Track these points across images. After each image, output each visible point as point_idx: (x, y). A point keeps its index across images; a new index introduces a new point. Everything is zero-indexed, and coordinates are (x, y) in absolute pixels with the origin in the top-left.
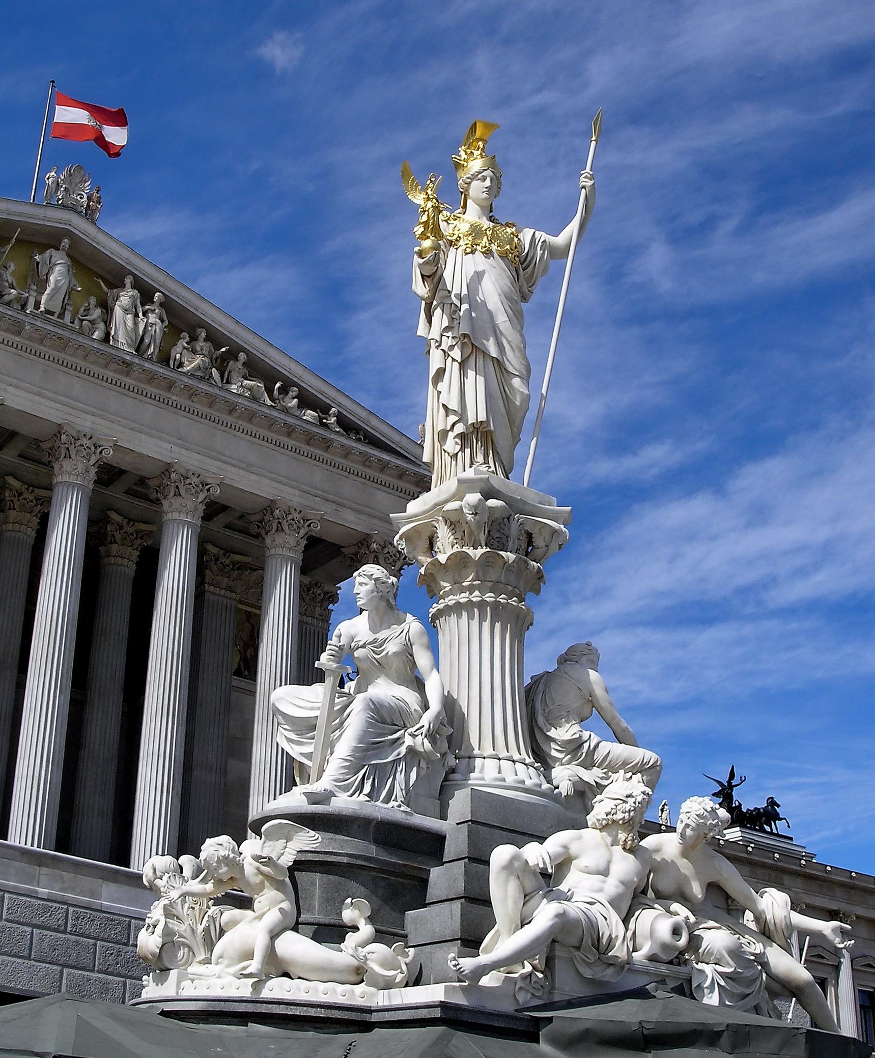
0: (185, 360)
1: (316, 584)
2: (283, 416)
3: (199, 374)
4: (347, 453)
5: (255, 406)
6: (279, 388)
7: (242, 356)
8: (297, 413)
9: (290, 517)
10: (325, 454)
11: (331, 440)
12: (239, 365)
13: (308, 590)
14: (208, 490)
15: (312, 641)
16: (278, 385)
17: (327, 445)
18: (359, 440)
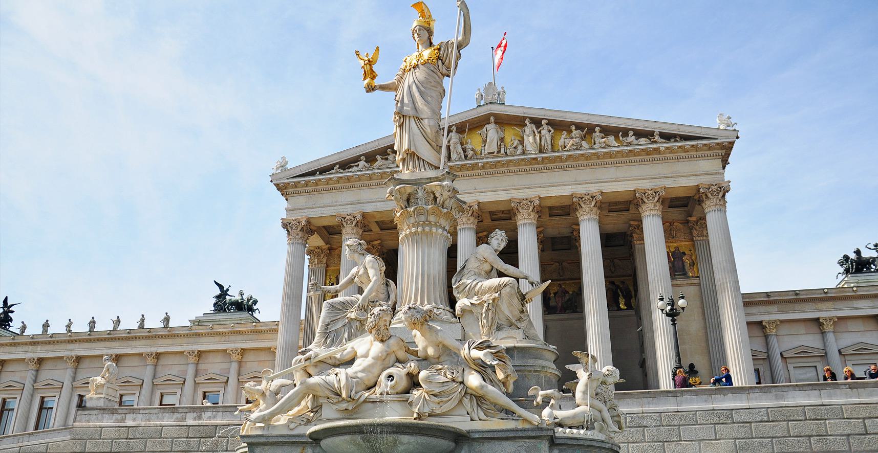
0: (566, 144)
1: (700, 219)
2: (626, 148)
3: (574, 147)
4: (671, 150)
5: (608, 150)
6: (621, 135)
7: (597, 129)
8: (636, 142)
9: (646, 194)
10: (660, 156)
11: (658, 148)
12: (598, 134)
13: (697, 224)
14: (596, 199)
15: (702, 249)
16: (620, 134)
17: (657, 150)
18: (676, 141)
